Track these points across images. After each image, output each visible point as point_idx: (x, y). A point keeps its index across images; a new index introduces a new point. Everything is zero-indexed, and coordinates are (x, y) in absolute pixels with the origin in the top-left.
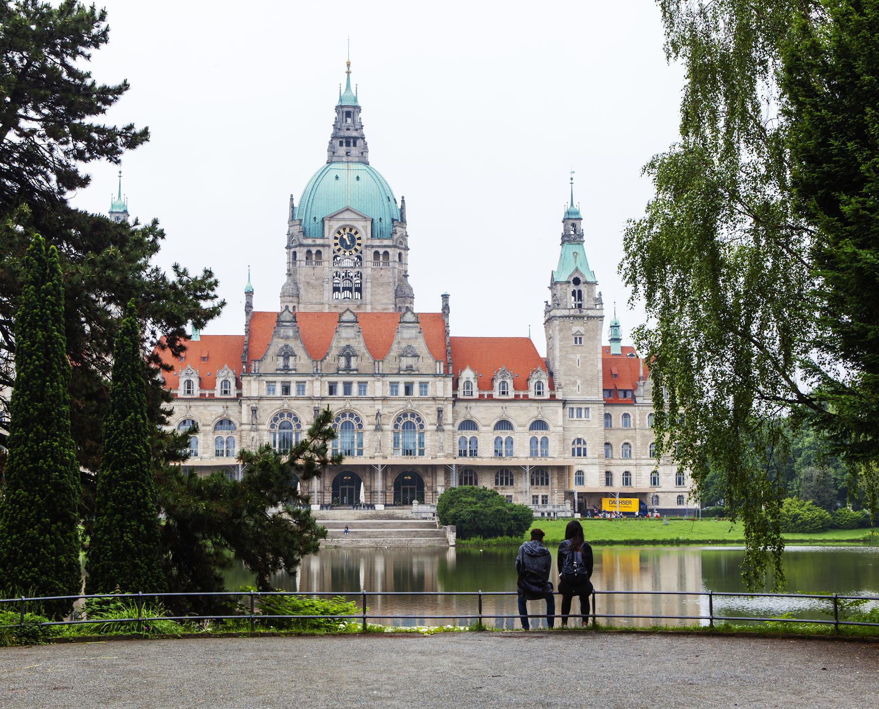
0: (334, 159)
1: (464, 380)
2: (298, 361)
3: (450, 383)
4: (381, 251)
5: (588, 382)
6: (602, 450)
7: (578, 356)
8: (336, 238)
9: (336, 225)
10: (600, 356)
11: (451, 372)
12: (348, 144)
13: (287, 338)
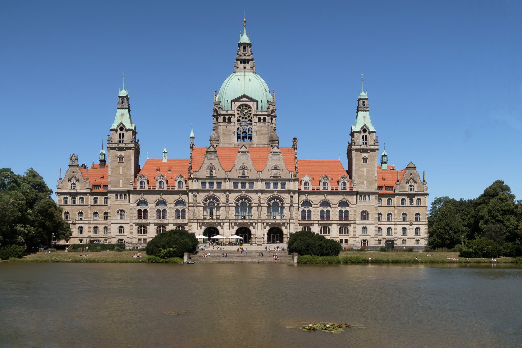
0: (237, 70)
1: (305, 181)
2: (217, 172)
4: (262, 117)
5: (370, 183)
7: (365, 169)
8: (238, 111)
9: (238, 104)
10: (376, 169)
12: (245, 63)
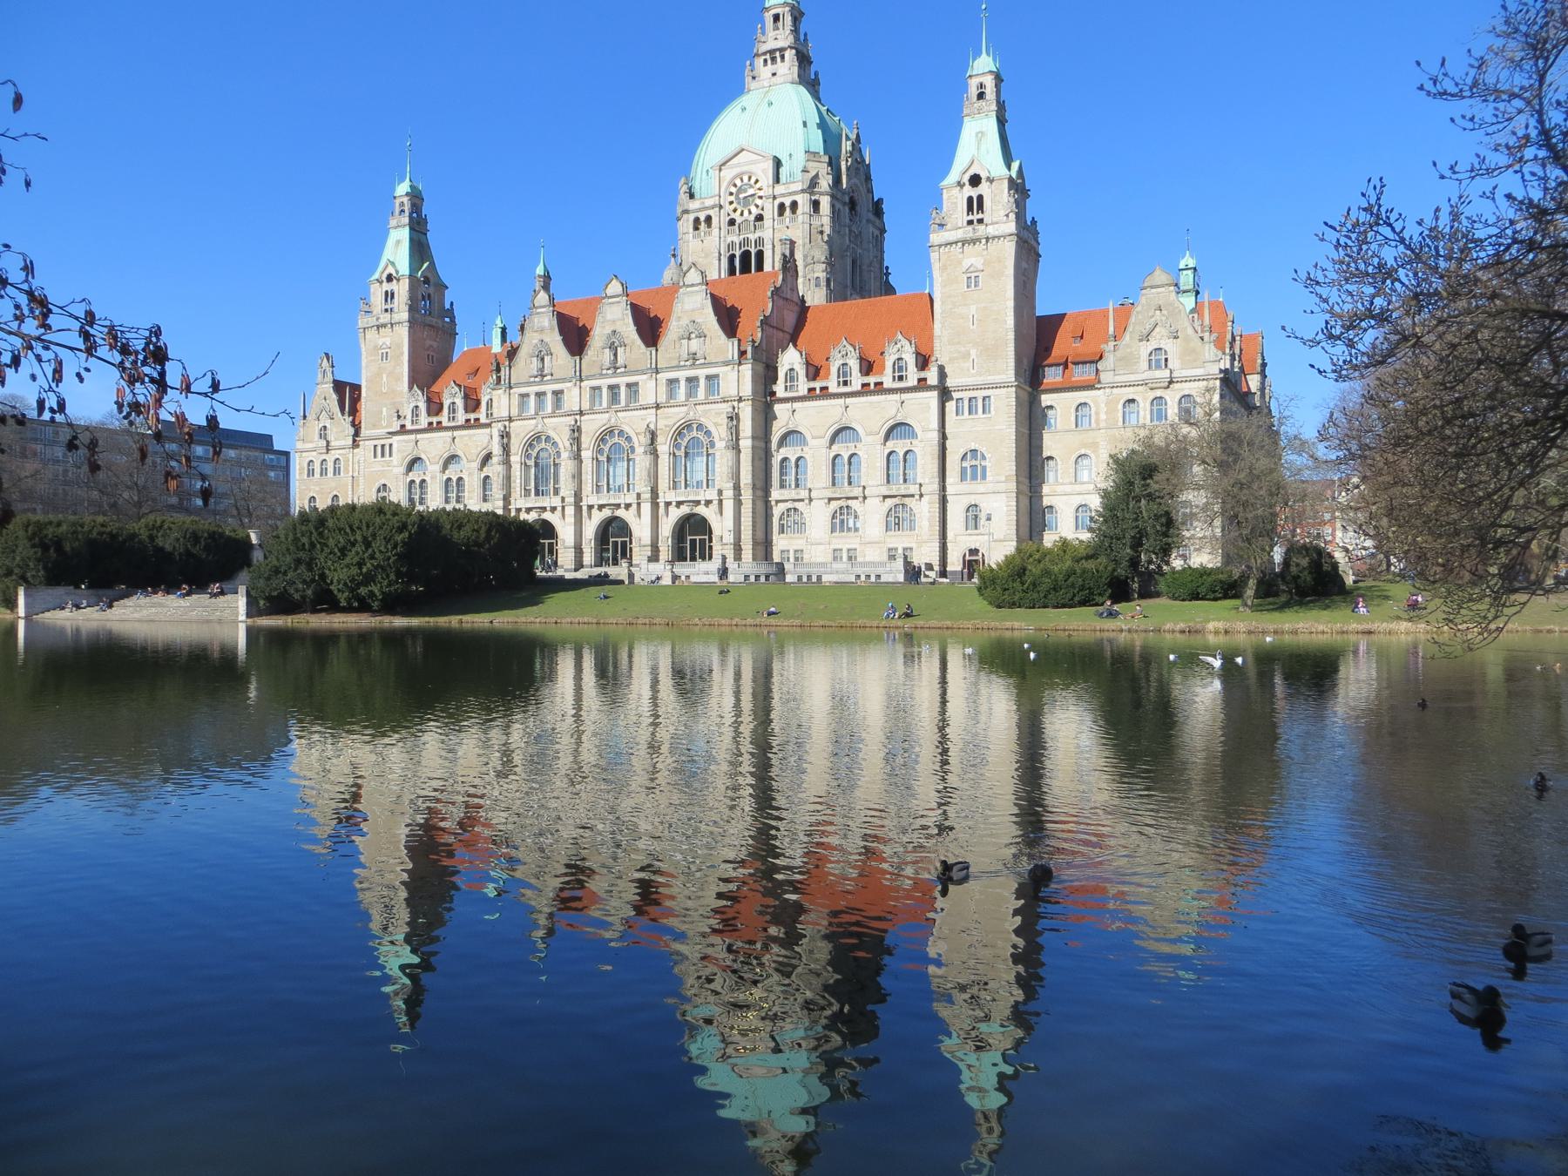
0: (753, 85)
1: (786, 367)
3: (747, 370)
6: (1010, 467)
7: (973, 309)
11: (749, 355)
12: (773, 60)
13: (542, 330)
